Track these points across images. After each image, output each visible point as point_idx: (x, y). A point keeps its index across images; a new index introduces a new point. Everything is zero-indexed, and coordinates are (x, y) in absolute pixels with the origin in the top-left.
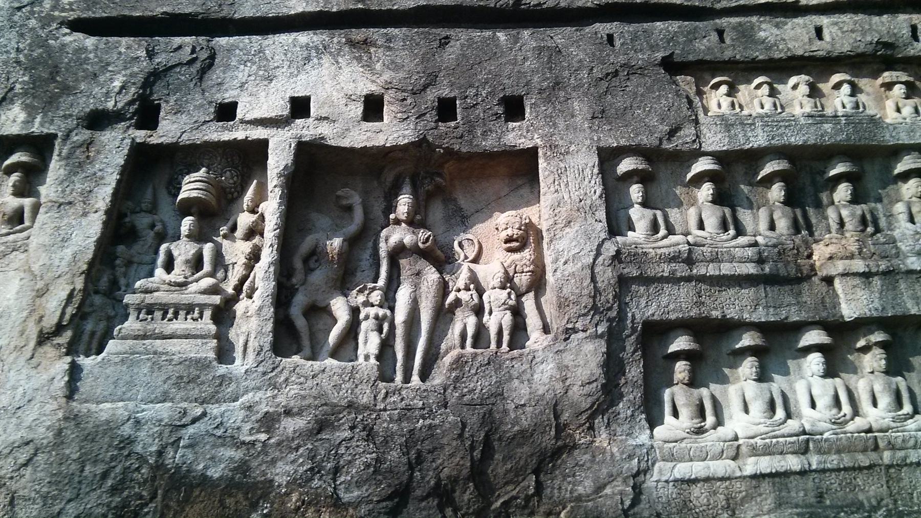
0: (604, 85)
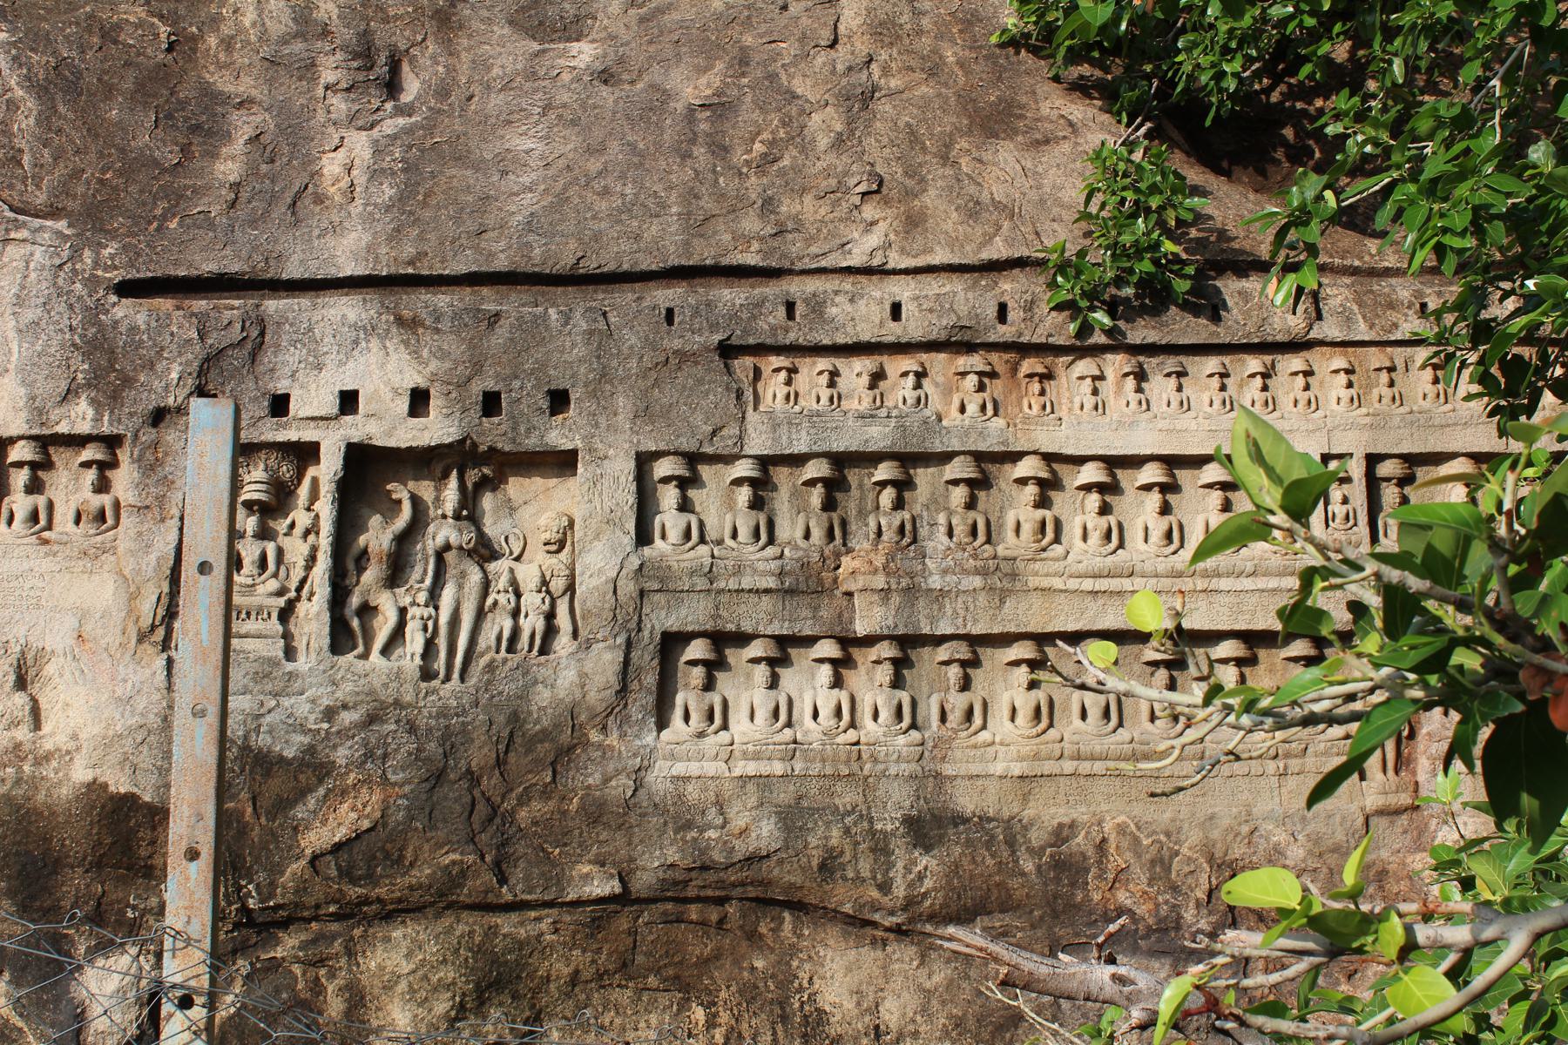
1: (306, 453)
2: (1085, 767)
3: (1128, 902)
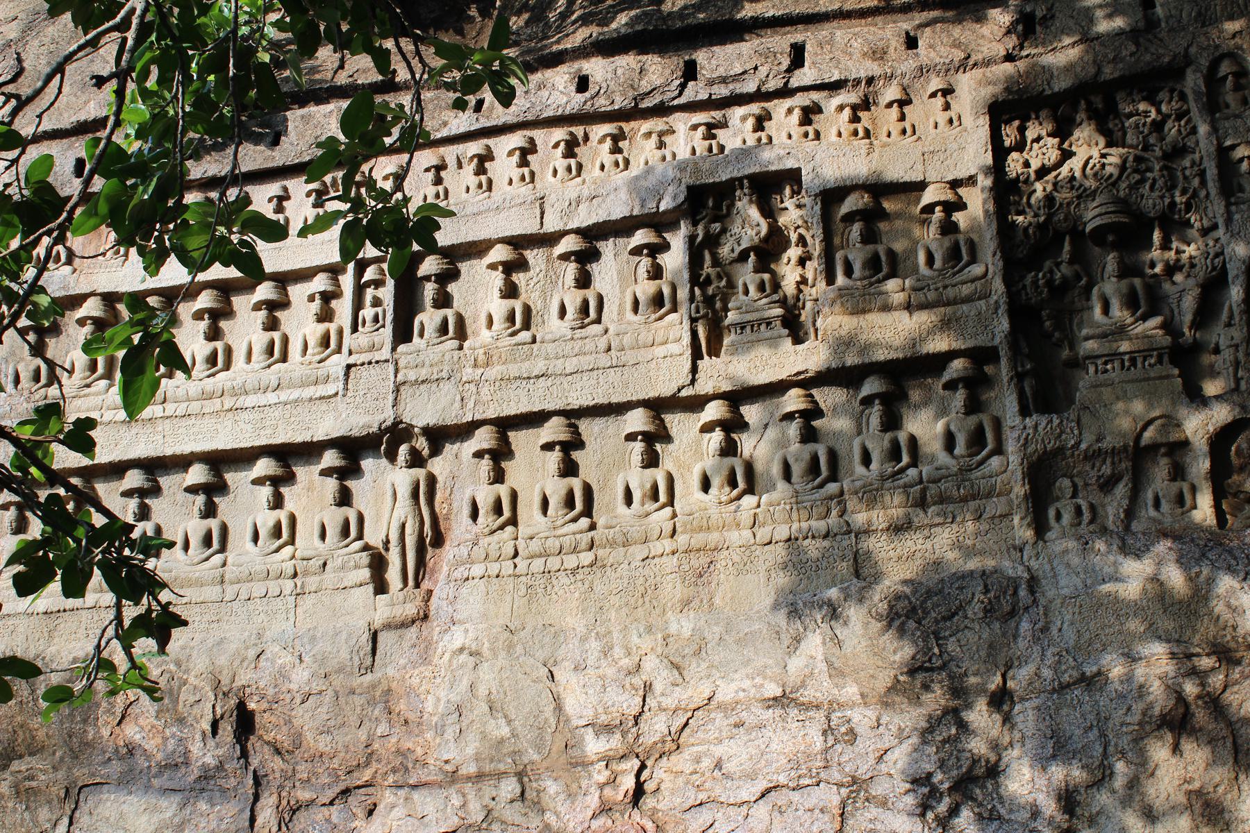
3: (138, 736)
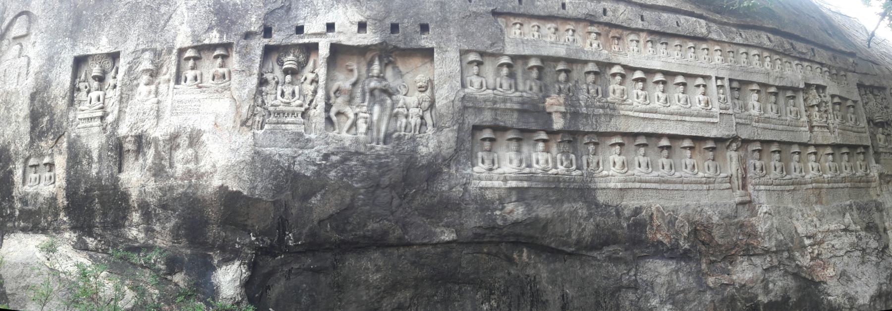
0: (465, 20)
1: (312, 48)
2: (644, 185)
